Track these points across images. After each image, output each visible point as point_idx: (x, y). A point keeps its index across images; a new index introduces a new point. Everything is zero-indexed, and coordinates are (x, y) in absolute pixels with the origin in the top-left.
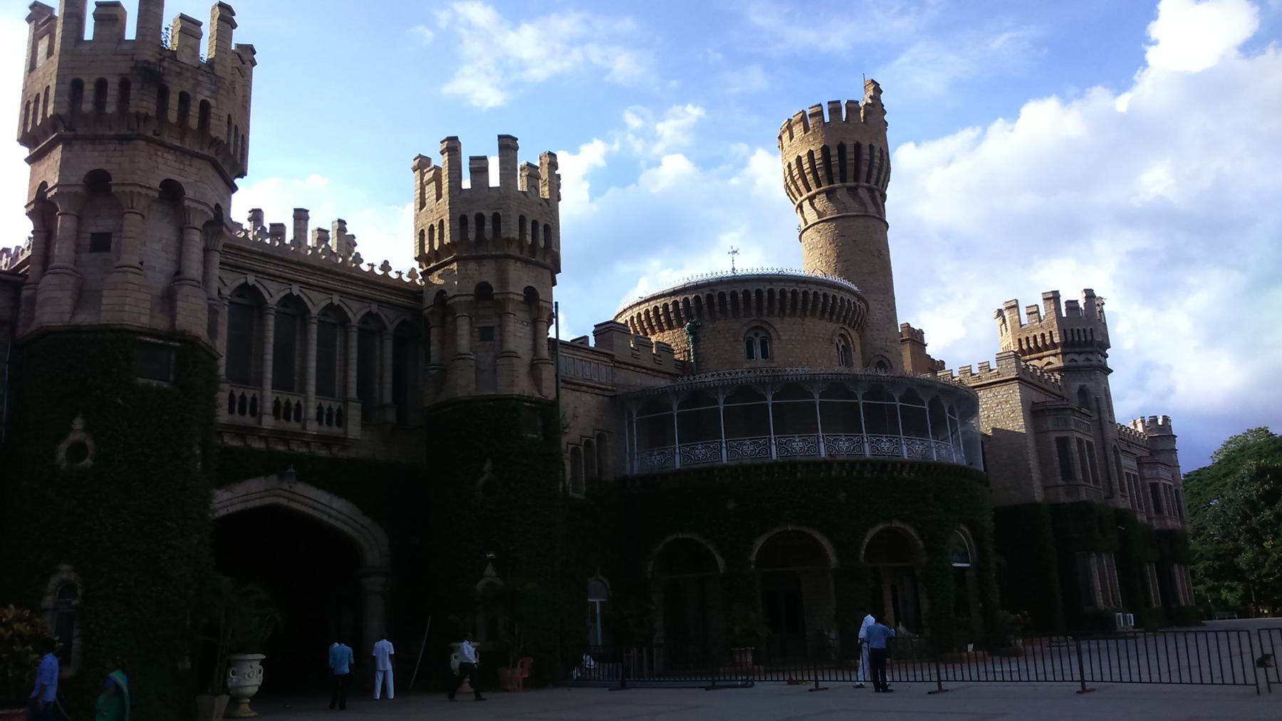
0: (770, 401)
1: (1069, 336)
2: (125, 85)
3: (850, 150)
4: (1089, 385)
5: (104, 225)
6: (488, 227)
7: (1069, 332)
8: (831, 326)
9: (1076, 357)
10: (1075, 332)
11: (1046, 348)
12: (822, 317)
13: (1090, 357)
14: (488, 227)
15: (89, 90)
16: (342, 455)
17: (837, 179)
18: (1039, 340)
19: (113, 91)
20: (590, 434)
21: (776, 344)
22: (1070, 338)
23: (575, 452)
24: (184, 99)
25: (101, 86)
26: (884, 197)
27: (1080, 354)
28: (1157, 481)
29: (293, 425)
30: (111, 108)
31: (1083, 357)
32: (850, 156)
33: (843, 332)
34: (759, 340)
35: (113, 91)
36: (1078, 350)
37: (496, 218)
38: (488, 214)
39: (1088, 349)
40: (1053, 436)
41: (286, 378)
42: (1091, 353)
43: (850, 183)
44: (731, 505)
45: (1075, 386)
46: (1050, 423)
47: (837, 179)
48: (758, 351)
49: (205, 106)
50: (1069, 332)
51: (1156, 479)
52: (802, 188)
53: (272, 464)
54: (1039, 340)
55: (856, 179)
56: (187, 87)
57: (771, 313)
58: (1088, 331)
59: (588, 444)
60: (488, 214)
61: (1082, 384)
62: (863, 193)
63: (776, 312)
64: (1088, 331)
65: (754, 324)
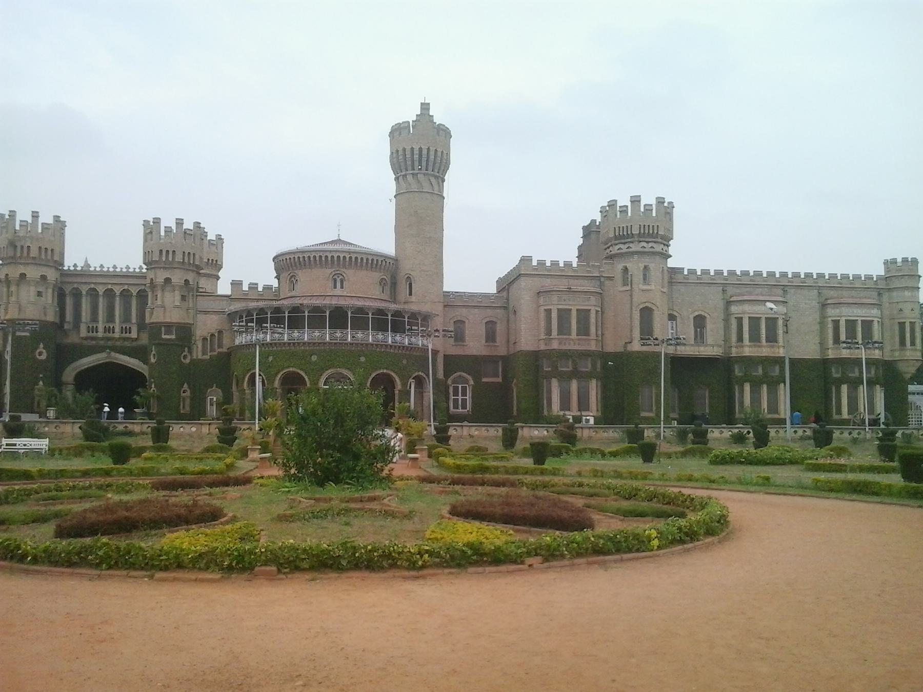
1: (617, 234)
4: (628, 265)
7: (617, 229)
8: (329, 271)
9: (621, 246)
10: (621, 229)
12: (321, 266)
13: (631, 245)
16: (134, 344)
20: (213, 331)
22: (617, 234)
23: (205, 339)
24: (22, 247)
27: (624, 243)
28: (839, 318)
29: (111, 335)
31: (627, 246)
32: (408, 156)
33: (338, 272)
36: (623, 241)
39: (629, 240)
40: (542, 308)
41: (110, 318)
42: (632, 242)
45: (620, 266)
46: (541, 300)
49: (29, 247)
50: (617, 229)
51: (838, 316)
53: (101, 349)
56: (22, 243)
57: (293, 269)
58: (629, 227)
59: (212, 335)
61: (624, 265)
62: (410, 178)
63: (299, 268)
64: (629, 227)
65: (291, 275)
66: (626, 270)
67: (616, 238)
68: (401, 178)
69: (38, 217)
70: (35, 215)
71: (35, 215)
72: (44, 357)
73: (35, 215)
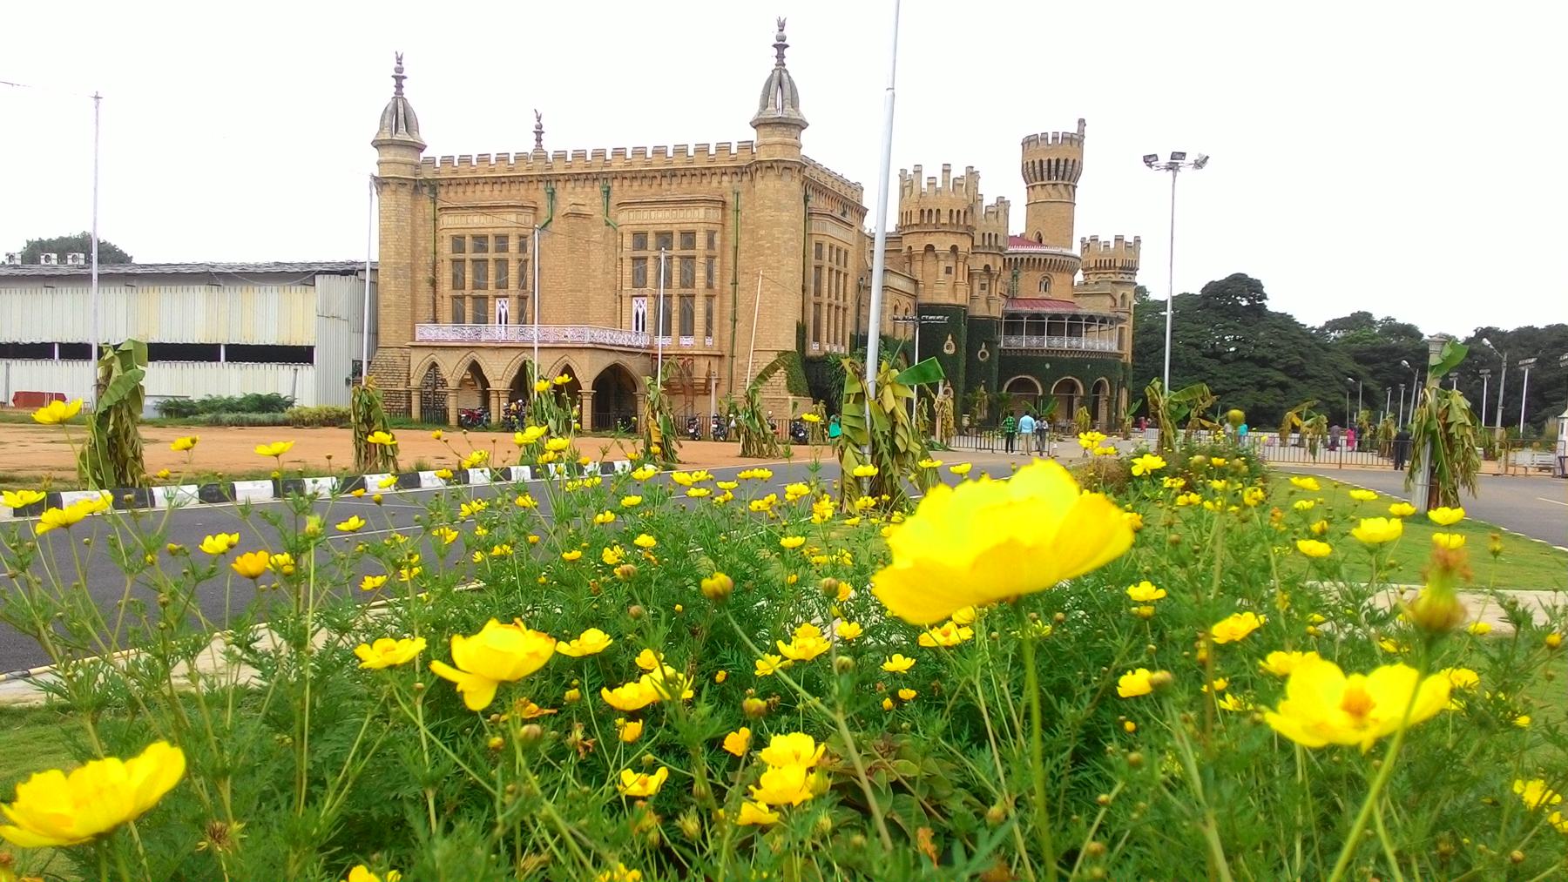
0: (1066, 321)
2: (965, 213)
3: (1070, 163)
4: (1128, 293)
5: (951, 264)
6: (993, 239)
11: (1110, 268)
14: (993, 239)
15: (955, 214)
17: (1060, 178)
18: (1108, 263)
19: (962, 214)
21: (1052, 286)
25: (958, 212)
26: (1074, 187)
30: (962, 223)
34: (1046, 284)
35: (962, 214)
37: (996, 235)
38: (993, 235)
43: (1066, 182)
44: (1048, 366)
47: (1060, 178)
48: (1043, 288)
52: (1039, 178)
54: (1108, 263)
55: (1069, 180)
60: (993, 235)
66: (1123, 296)
67: (1120, 268)
68: (1061, 188)
69: (949, 171)
70: (947, 168)
71: (946, 169)
72: (951, 351)
73: (946, 169)
